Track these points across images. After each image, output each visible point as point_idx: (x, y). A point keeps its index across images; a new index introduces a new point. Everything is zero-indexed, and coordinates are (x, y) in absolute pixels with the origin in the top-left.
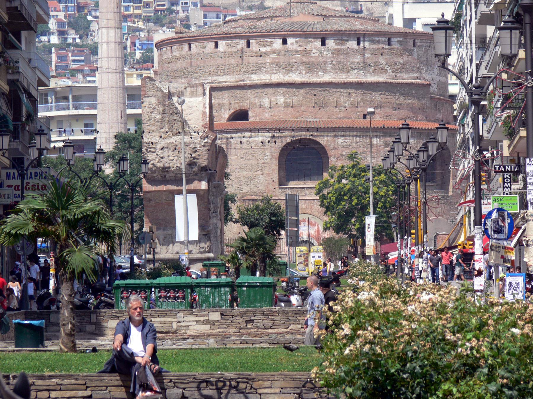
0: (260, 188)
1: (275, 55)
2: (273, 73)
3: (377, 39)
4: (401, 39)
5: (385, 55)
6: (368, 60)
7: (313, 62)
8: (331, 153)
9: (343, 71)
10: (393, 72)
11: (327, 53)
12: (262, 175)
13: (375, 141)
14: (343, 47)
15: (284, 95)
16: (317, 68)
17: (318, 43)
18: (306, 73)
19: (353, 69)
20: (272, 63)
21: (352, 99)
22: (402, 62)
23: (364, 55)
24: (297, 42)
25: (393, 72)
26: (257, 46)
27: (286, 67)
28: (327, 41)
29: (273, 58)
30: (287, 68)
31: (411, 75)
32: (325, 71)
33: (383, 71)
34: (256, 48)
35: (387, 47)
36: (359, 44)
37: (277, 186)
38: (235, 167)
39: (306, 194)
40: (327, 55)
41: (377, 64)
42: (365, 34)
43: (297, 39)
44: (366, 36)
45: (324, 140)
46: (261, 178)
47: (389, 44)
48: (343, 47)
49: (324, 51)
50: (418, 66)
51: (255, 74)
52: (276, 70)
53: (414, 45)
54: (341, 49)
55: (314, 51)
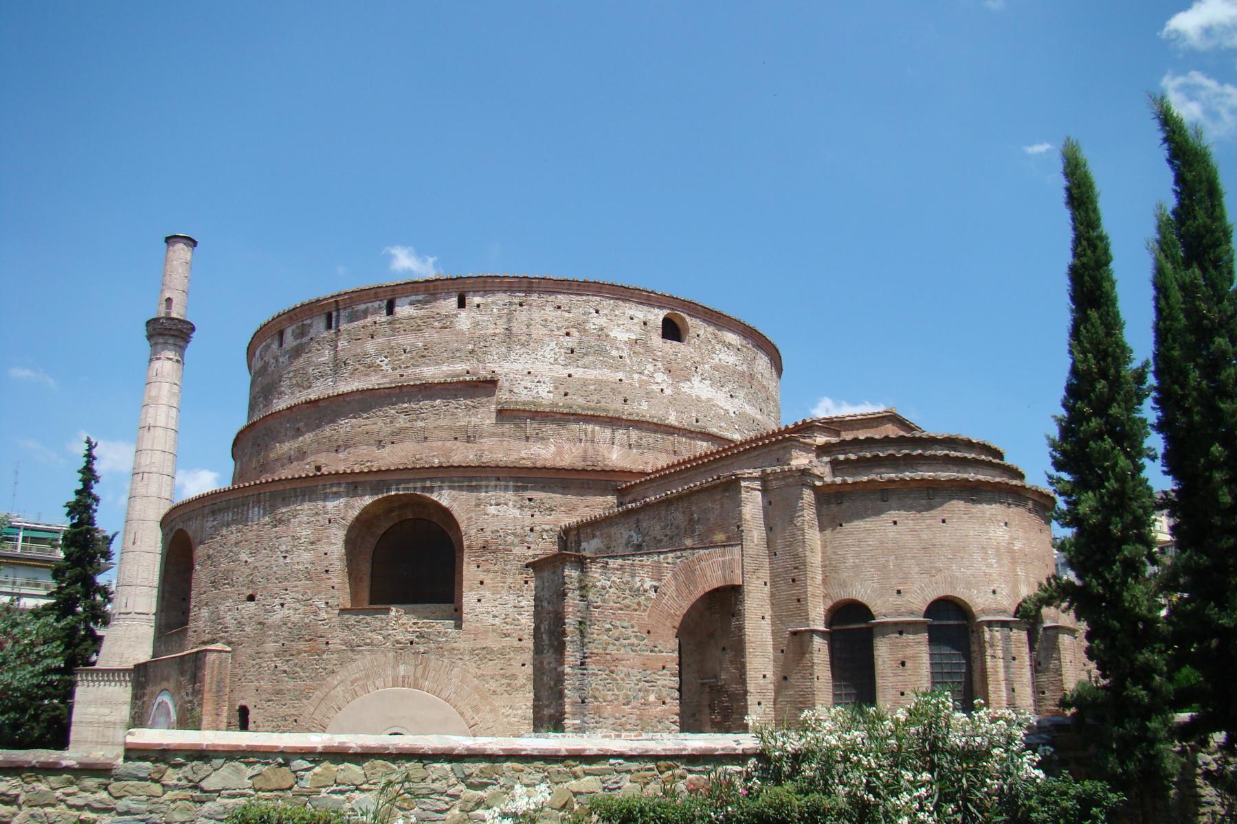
3: (362, 307)
4: (420, 297)
5: (379, 338)
6: (342, 354)
10: (394, 369)
17: (275, 346)
22: (421, 344)
23: (336, 346)
25: (394, 369)
31: (445, 368)
33: (374, 368)
36: (329, 327)
41: (359, 358)
42: (336, 302)
44: (341, 305)
47: (390, 311)
50: (470, 347)
53: (462, 304)
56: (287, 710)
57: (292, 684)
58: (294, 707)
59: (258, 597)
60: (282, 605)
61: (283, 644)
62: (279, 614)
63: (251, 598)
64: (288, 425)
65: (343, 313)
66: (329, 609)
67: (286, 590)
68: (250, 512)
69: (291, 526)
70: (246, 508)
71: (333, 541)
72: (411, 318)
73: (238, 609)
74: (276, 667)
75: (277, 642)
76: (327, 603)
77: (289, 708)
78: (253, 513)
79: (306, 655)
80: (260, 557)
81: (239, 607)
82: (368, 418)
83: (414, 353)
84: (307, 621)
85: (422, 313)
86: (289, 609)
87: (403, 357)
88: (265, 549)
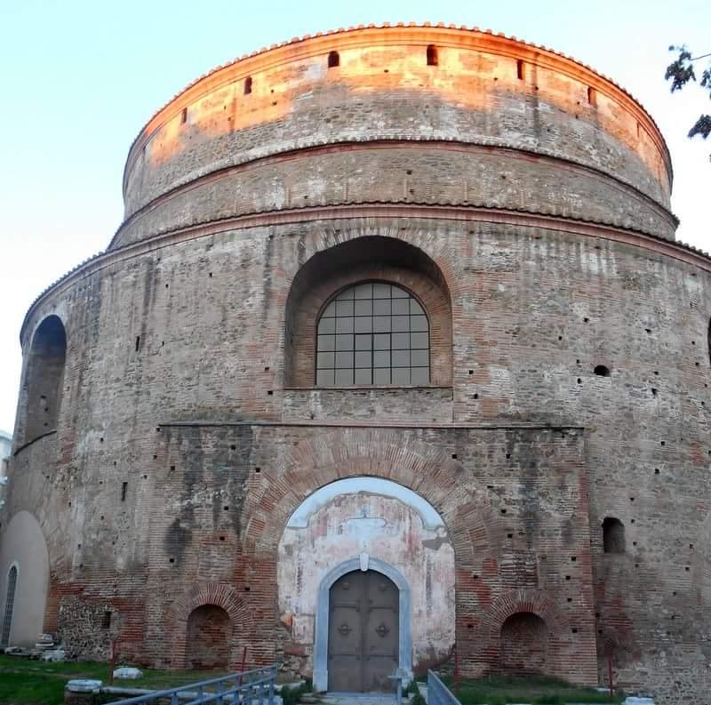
0: (226, 392)
1: (309, 95)
2: (304, 135)
3: (564, 78)
4: (616, 105)
6: (544, 117)
7: (405, 101)
8: (460, 285)
9: (485, 129)
11: (443, 83)
12: (235, 352)
13: (593, 262)
14: (483, 75)
15: (324, 175)
16: (415, 115)
18: (386, 127)
19: (510, 129)
20: (301, 114)
21: (510, 190)
23: (535, 104)
24: (365, 58)
25: (603, 165)
26: (268, 83)
27: (336, 117)
28: (441, 55)
29: (303, 103)
30: (339, 119)
32: (436, 124)
34: (265, 89)
35: (588, 106)
36: (520, 76)
37: (276, 386)
38: (161, 338)
39: (372, 411)
40: (440, 85)
43: (365, 51)
45: (435, 242)
46: (231, 363)
48: (483, 75)
49: (435, 76)
51: (259, 145)
52: (310, 127)
54: (479, 79)
55: (408, 76)
56: (681, 532)
57: (680, 499)
58: (687, 528)
59: (614, 373)
60: (654, 391)
61: (663, 443)
62: (653, 404)
63: (601, 371)
64: (483, 166)
65: (540, 71)
66: (706, 411)
67: (656, 373)
68: (583, 257)
69: (652, 295)
70: (574, 248)
71: (700, 332)
72: (609, 120)
73: (579, 381)
74: (657, 471)
75: (654, 439)
76: (703, 403)
77: (682, 528)
78: (588, 257)
79: (691, 462)
80: (610, 320)
81: (583, 378)
82: (599, 204)
83: (617, 158)
84: (685, 419)
85: (617, 121)
86: (664, 400)
87: (608, 156)
88: (617, 311)
